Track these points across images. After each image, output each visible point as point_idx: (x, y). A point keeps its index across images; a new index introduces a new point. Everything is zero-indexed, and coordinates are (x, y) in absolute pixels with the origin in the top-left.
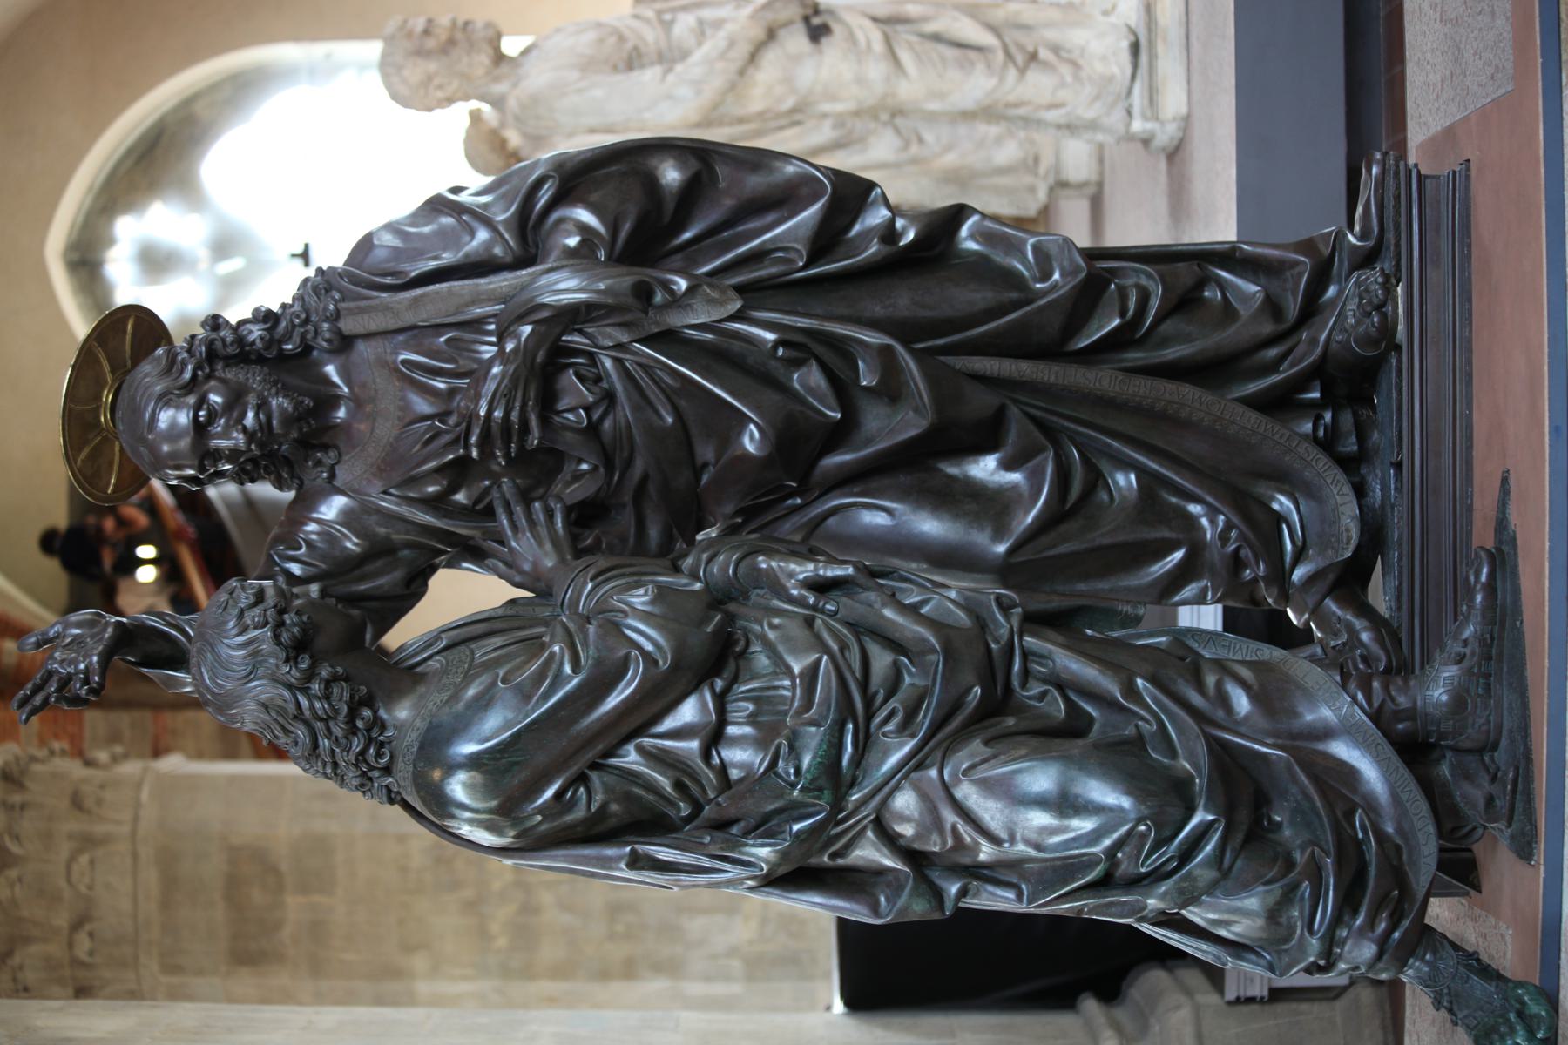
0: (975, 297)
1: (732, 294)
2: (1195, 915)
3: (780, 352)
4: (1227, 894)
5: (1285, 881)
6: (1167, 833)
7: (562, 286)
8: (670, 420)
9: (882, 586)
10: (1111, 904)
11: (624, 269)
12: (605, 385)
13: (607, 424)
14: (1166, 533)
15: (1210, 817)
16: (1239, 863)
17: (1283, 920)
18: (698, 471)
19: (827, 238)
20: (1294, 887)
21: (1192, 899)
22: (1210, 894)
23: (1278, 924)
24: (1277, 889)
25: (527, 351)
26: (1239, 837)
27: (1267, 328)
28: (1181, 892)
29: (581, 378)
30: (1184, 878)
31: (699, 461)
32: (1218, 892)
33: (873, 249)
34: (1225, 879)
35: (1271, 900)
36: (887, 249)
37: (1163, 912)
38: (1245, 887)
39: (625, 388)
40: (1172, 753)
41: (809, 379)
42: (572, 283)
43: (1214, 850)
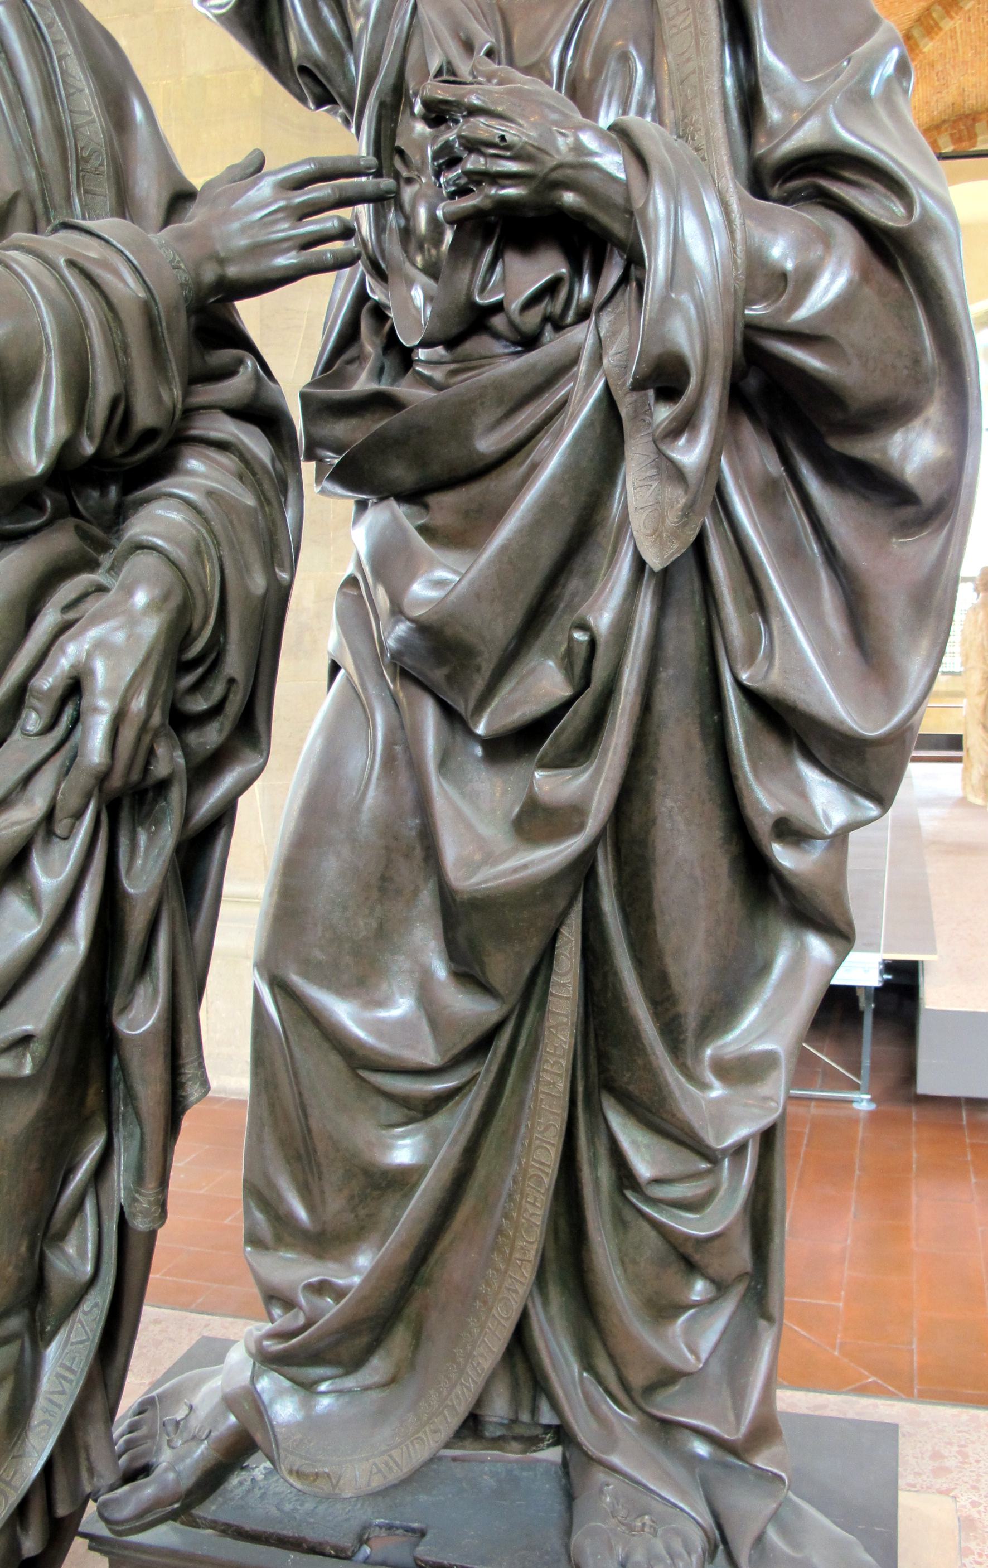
0: (692, 960)
1: (676, 548)
3: (580, 636)
7: (690, 226)
8: (488, 444)
9: (78, 815)
11: (722, 348)
12: (548, 332)
13: (499, 347)
18: (414, 496)
19: (784, 722)
25: (577, 172)
27: (638, 1379)
29: (551, 288)
31: (433, 500)
33: (765, 799)
36: (762, 827)
39: (533, 367)
41: (543, 683)
42: (698, 251)
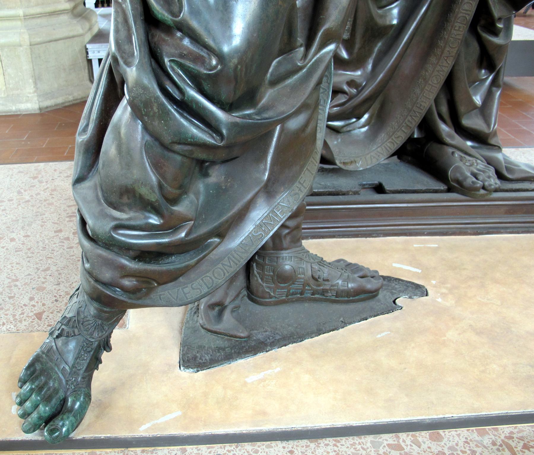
2: (123, 112)
4: (147, 148)
5: (162, 201)
6: (207, 87)
10: (129, 29)
14: (356, 50)
15: (224, 132)
16: (179, 158)
17: (125, 200)
20: (157, 211)
21: (138, 111)
22: (145, 128)
23: (121, 195)
24: (154, 197)
26: (201, 155)
28: (147, 104)
30: (161, 106)
32: (147, 138)
34: (161, 145)
35: (144, 191)
37: (123, 82)
38: (157, 166)
40: (273, 83)
43: (193, 137)
